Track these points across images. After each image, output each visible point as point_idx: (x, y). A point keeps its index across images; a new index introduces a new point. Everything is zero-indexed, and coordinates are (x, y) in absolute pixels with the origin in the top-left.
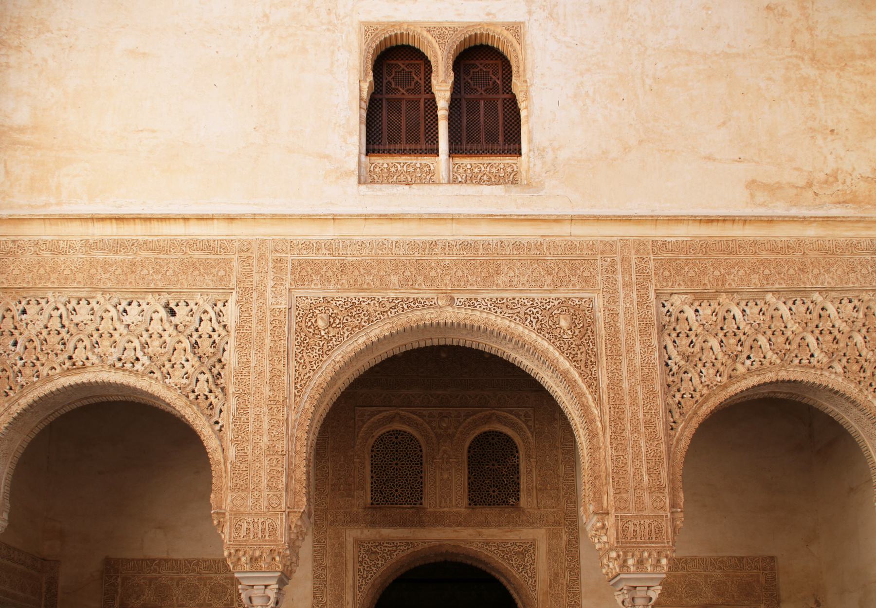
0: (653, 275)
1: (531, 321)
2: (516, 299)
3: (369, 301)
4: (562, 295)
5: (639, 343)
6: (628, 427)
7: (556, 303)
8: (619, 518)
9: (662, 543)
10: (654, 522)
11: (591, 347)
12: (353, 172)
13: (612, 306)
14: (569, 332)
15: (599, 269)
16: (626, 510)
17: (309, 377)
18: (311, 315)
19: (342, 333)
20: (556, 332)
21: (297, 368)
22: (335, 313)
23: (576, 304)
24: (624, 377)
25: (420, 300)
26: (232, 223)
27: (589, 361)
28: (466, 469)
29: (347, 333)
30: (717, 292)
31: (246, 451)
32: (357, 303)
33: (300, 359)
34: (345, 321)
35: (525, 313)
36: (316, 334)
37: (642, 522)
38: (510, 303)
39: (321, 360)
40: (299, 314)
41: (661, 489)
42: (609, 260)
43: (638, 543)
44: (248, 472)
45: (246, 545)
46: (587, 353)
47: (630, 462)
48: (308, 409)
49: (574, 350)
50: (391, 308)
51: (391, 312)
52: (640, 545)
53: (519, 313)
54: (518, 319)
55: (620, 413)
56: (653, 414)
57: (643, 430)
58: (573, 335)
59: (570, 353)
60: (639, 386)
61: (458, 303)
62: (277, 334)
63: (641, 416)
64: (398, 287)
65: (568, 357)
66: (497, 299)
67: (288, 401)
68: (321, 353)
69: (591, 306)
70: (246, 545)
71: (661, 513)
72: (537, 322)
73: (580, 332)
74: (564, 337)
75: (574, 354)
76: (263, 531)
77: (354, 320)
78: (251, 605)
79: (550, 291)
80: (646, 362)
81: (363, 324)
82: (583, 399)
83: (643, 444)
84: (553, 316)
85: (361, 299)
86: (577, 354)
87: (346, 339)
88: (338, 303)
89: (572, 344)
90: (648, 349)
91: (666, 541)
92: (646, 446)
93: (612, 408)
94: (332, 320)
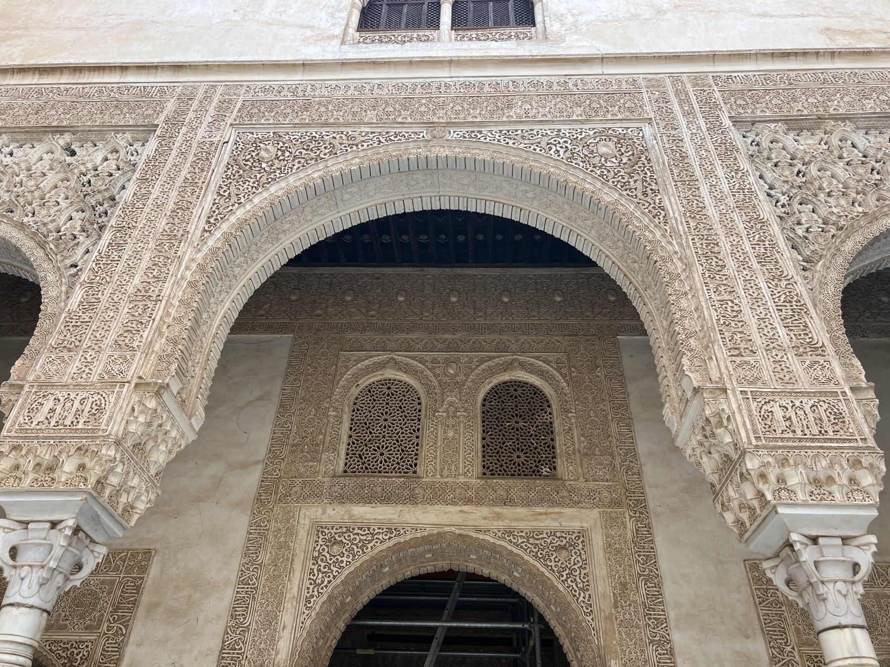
0: (723, 105)
1: (556, 150)
2: (535, 131)
3: (334, 135)
4: (599, 126)
5: (721, 167)
6: (731, 263)
7: (591, 133)
8: (749, 396)
9: (850, 441)
10: (821, 403)
11: (649, 174)
12: (337, 36)
13: (673, 132)
14: (614, 160)
15: (646, 100)
16: (759, 383)
17: (231, 210)
18: (253, 149)
19: (290, 166)
20: (596, 161)
21: (217, 201)
22: (287, 147)
23: (620, 134)
24: (706, 203)
25: (404, 133)
26: (179, 71)
27: (648, 189)
28: (479, 426)
29: (297, 166)
30: (820, 118)
31: (100, 296)
32: (318, 136)
33: (225, 191)
34: (297, 153)
35: (548, 144)
36: (255, 167)
37: (797, 403)
38: (526, 134)
39: (254, 193)
40: (237, 148)
41: (817, 349)
42: (657, 93)
43: (800, 440)
44: (90, 324)
45: (37, 438)
46: (644, 181)
47: (746, 310)
48: (219, 248)
49: (624, 178)
50: (363, 141)
51: (362, 146)
52: (803, 444)
53: (539, 143)
54: (538, 149)
55: (712, 245)
56: (768, 246)
57: (756, 266)
58: (619, 163)
59: (618, 181)
60: (734, 213)
61: (455, 136)
62: (199, 166)
63: (747, 247)
64: (375, 121)
65: (616, 186)
66: (508, 131)
67: (189, 236)
68: (255, 185)
69: (641, 135)
70: (37, 438)
71: (830, 387)
72: (565, 152)
73: (630, 160)
74: (606, 165)
75: (624, 183)
76: (78, 413)
77: (309, 152)
78: (11, 562)
79: (581, 122)
80: (737, 187)
81: (322, 156)
82: (647, 233)
83: (762, 285)
84: (588, 146)
85: (324, 133)
86: (629, 182)
87: (294, 171)
88: (292, 137)
89: (619, 172)
90: (737, 174)
91: (857, 437)
92: (769, 288)
93: (696, 240)
94: (280, 153)
